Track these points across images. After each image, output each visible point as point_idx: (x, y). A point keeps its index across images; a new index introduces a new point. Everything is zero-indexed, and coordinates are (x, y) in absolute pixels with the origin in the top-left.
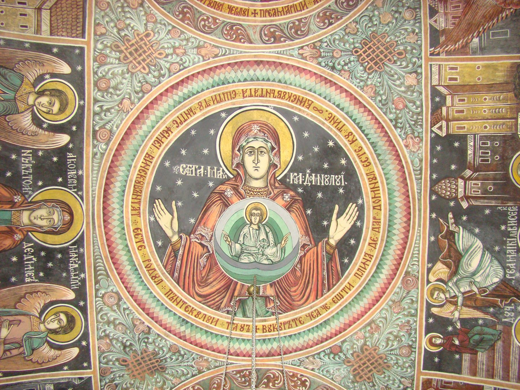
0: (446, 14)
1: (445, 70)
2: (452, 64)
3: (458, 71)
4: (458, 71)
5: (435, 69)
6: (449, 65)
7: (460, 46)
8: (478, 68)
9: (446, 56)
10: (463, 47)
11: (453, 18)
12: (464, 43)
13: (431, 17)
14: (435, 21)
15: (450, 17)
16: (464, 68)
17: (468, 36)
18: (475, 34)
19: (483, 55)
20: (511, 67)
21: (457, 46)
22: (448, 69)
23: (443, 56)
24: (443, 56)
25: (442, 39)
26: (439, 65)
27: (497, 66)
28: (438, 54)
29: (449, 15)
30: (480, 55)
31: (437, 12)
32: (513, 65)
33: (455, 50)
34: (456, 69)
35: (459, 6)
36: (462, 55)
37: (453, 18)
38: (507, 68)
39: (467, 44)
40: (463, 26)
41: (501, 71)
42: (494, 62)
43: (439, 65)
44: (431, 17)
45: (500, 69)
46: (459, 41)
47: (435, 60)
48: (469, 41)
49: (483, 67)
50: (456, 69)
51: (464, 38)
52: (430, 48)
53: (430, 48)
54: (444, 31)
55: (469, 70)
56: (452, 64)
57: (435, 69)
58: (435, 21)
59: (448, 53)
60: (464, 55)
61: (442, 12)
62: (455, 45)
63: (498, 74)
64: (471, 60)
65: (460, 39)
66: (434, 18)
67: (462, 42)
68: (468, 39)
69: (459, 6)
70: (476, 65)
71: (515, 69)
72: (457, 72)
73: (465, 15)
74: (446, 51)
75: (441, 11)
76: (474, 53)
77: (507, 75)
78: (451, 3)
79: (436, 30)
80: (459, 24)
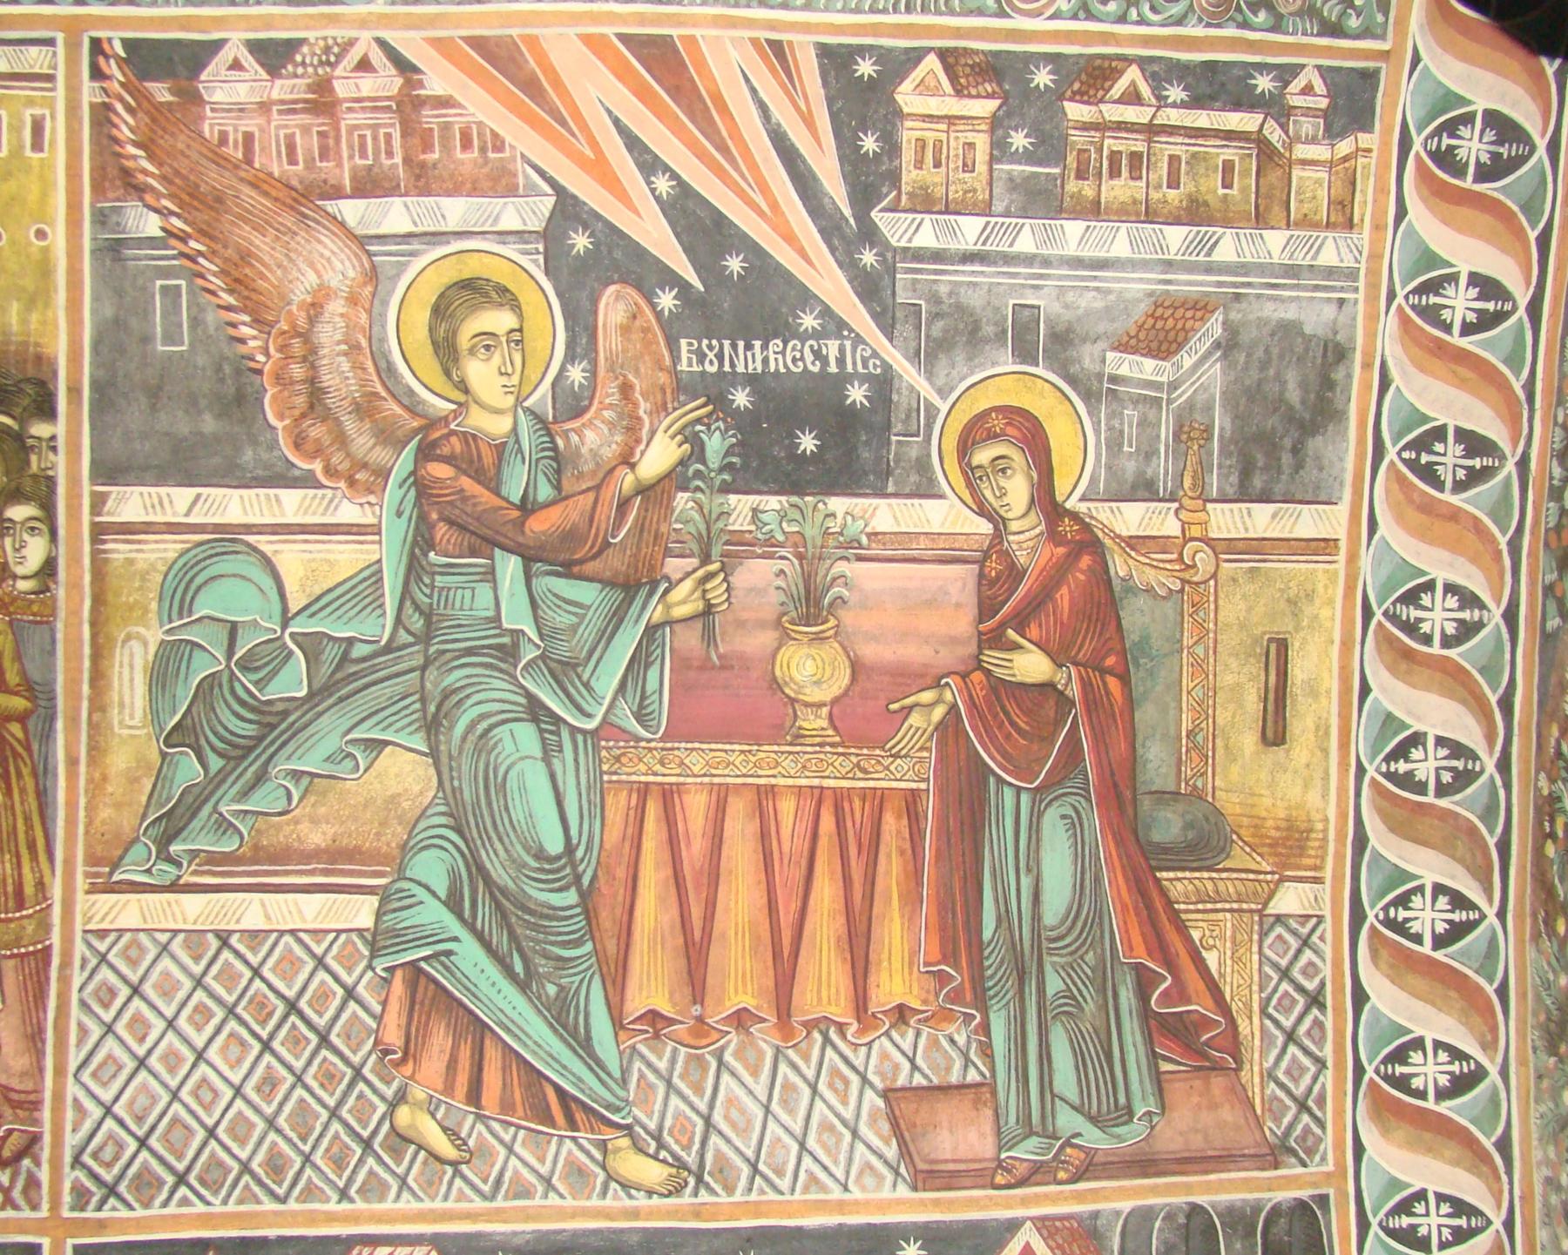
0: (264, 107)
1: (30, 102)
2: (57, 130)
3: (28, 153)
4: (28, 153)
5: (35, 58)
6: (53, 117)
7: (130, 164)
8: (41, 234)
9: (92, 106)
10: (126, 173)
11: (249, 138)
12: (141, 177)
13: (256, 48)
14: (236, 65)
15: (251, 124)
16: (42, 178)
17: (172, 197)
18: (175, 221)
19: (93, 252)
20: (39, 358)
21: (132, 150)
22: (38, 111)
23: (89, 93)
24: (89, 93)
25: (161, 92)
26: (50, 78)
27: (47, 305)
28: (97, 74)
29: (261, 121)
30: (94, 239)
31: (274, 71)
32: (44, 362)
33: (116, 141)
34: (37, 145)
35: (292, 161)
36: (92, 170)
37: (249, 138)
38: (37, 345)
39: (140, 190)
40: (213, 178)
41: (24, 322)
42: (61, 297)
43: (50, 78)
44: (256, 48)
45: (35, 317)
46: (151, 157)
47: (72, 62)
48: (149, 198)
49: (46, 251)
50: (37, 145)
51: (164, 178)
52: (125, 42)
53: (125, 42)
54: (192, 98)
55: (33, 195)
56: (57, 130)
57: (35, 58)
58: (236, 65)
59: (102, 114)
60: (93, 179)
61: (275, 95)
62: (136, 144)
63: (15, 308)
64: (74, 206)
65: (160, 165)
66: (248, 60)
67: (145, 172)
68: (159, 195)
69: (292, 161)
70: (52, 224)
71: (31, 371)
72: (21, 147)
73: (254, 186)
74: (108, 107)
75: (280, 90)
76: (101, 219)
77: (8, 343)
78: (306, 130)
79: (202, 66)
80: (220, 161)
